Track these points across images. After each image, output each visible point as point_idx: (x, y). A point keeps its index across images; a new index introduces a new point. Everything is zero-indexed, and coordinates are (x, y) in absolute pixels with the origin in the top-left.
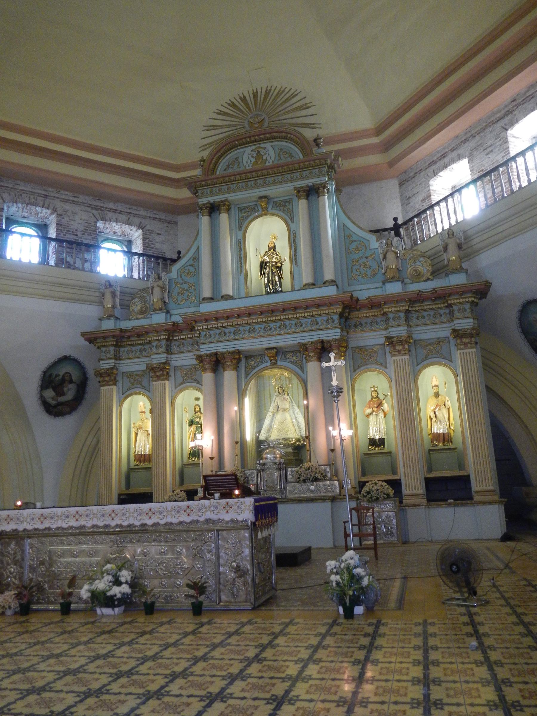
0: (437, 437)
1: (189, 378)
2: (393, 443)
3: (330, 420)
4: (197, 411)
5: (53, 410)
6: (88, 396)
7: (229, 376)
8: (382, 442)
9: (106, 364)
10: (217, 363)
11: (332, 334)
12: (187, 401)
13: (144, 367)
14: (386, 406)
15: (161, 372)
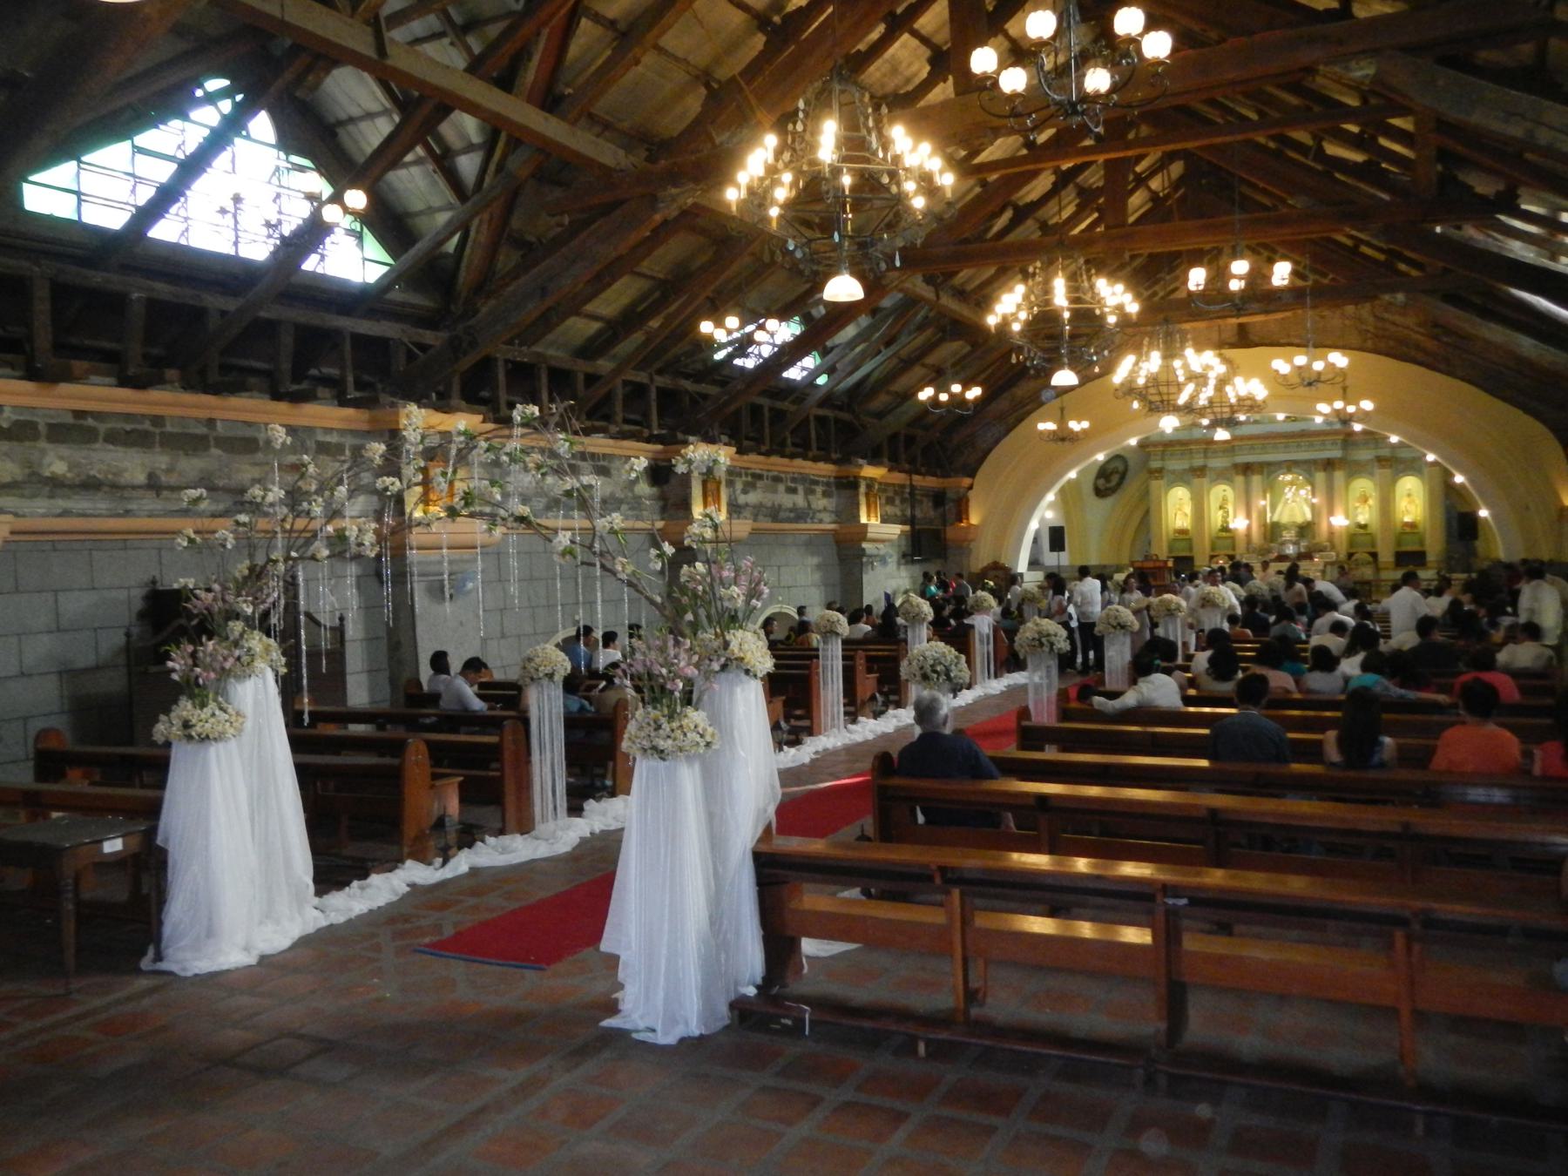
0: (1407, 524)
1: (1223, 476)
2: (1375, 526)
3: (1331, 513)
4: (1225, 500)
5: (1100, 493)
6: (1126, 482)
7: (1256, 480)
8: (1364, 527)
9: (1155, 464)
10: (1247, 469)
11: (1336, 453)
12: (1221, 493)
13: (1186, 466)
14: (1371, 502)
15: (1200, 471)
